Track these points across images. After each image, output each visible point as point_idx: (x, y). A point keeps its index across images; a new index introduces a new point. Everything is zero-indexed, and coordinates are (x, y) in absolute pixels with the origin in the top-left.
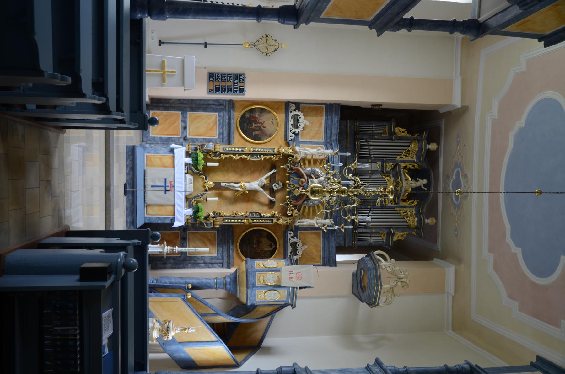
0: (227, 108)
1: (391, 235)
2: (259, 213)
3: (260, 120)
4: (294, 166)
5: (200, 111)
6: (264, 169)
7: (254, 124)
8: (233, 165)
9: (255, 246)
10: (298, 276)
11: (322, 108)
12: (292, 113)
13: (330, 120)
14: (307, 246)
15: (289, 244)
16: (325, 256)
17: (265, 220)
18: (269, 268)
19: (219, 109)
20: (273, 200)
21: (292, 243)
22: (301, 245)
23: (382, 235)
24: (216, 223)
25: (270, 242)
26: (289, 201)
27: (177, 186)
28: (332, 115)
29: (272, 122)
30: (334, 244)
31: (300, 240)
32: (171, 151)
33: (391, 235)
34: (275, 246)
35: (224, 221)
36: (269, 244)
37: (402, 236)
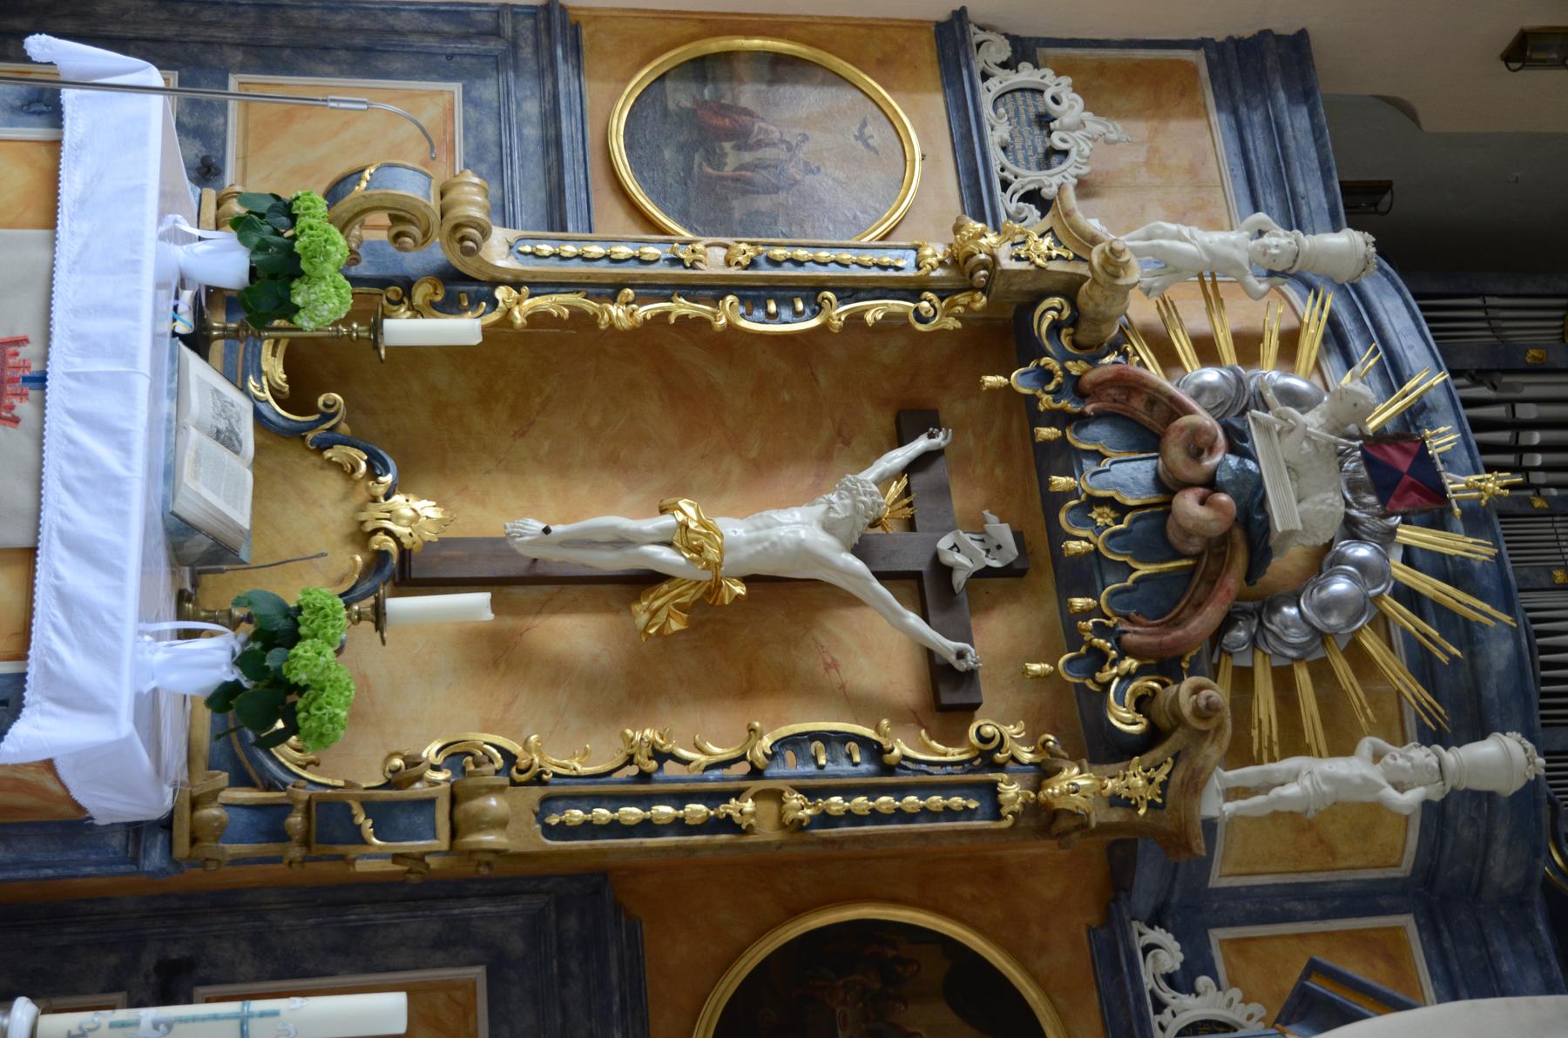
0: (527, 52)
2: (863, 741)
3: (772, 128)
4: (1093, 361)
5: (330, 69)
6: (847, 443)
7: (733, 148)
8: (595, 420)
11: (1192, 70)
12: (991, 83)
13: (1259, 132)
17: (924, 789)
19: (467, 61)
20: (961, 655)
24: (475, 805)
26: (1101, 630)
27: (74, 376)
28: (1269, 96)
29: (861, 137)
31: (1246, 1000)
32: (30, 103)
35: (554, 820)
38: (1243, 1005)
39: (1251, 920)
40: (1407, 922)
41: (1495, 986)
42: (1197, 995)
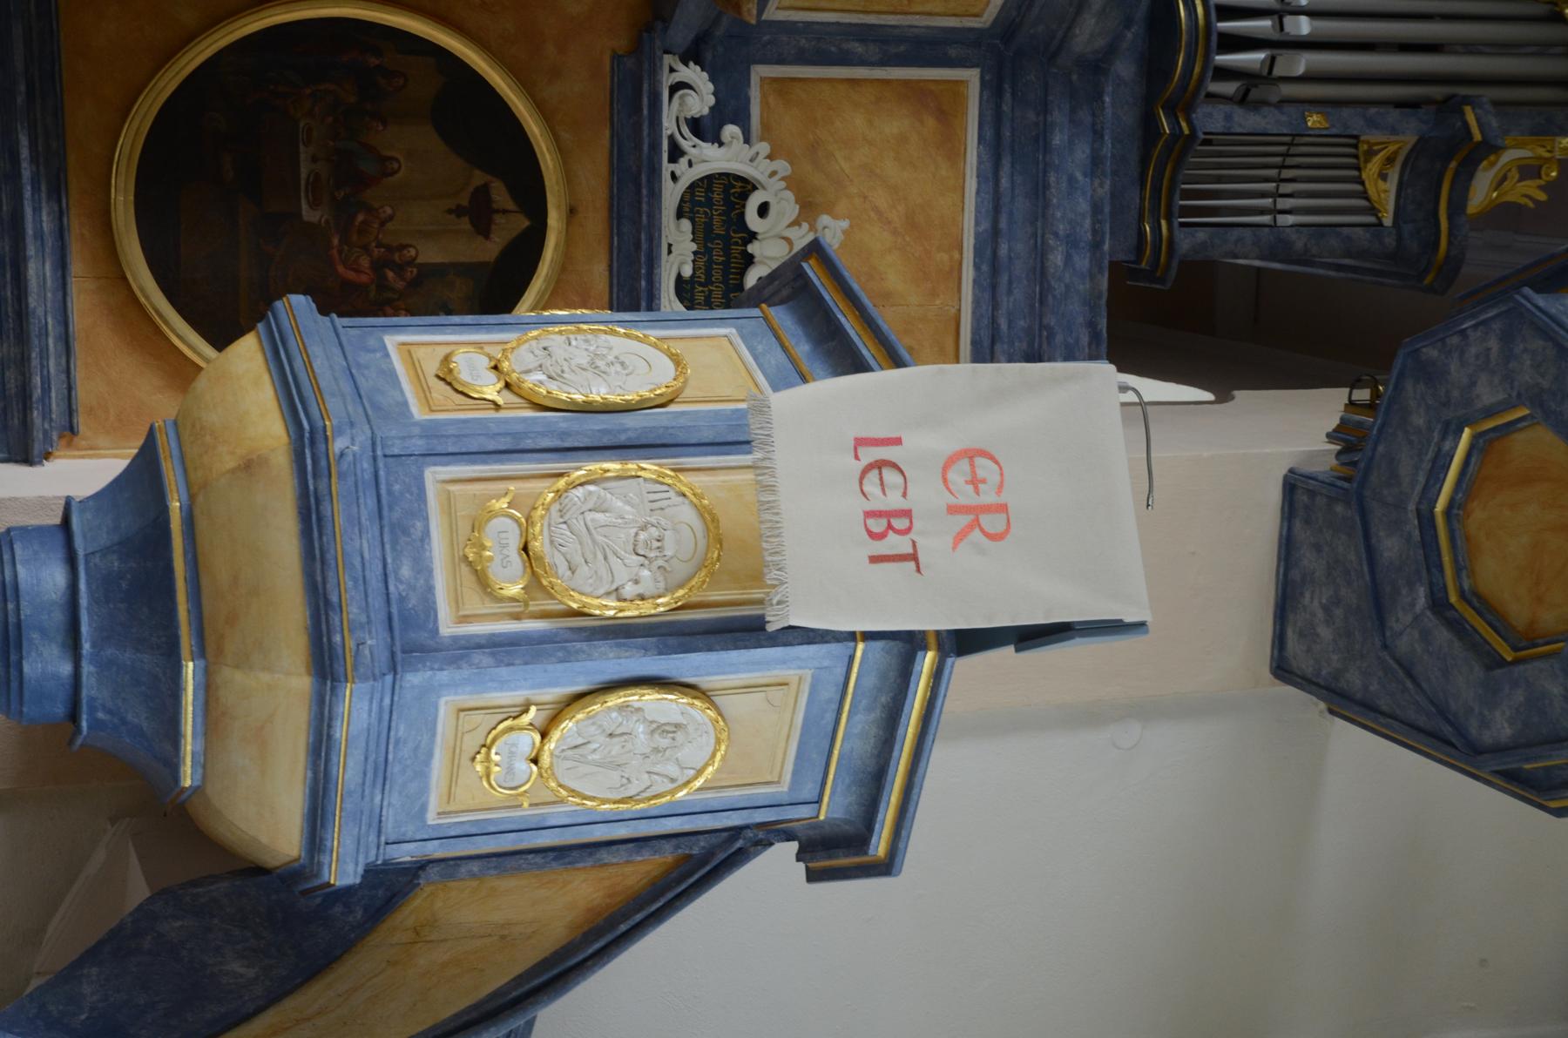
1: (1453, 165)
9: (309, 214)
10: (967, 496)
14: (845, 224)
15: (671, 195)
16: (994, 320)
18: (588, 409)
21: (692, 187)
22: (785, 206)
23: (1371, 169)
25: (479, 178)
30: (1084, 206)
33: (1453, 165)
34: (526, 223)
36: (465, 202)
37: (1529, 171)
38: (768, 161)
39: (802, 59)
40: (972, 76)
41: (1041, 157)
42: (721, 144)
